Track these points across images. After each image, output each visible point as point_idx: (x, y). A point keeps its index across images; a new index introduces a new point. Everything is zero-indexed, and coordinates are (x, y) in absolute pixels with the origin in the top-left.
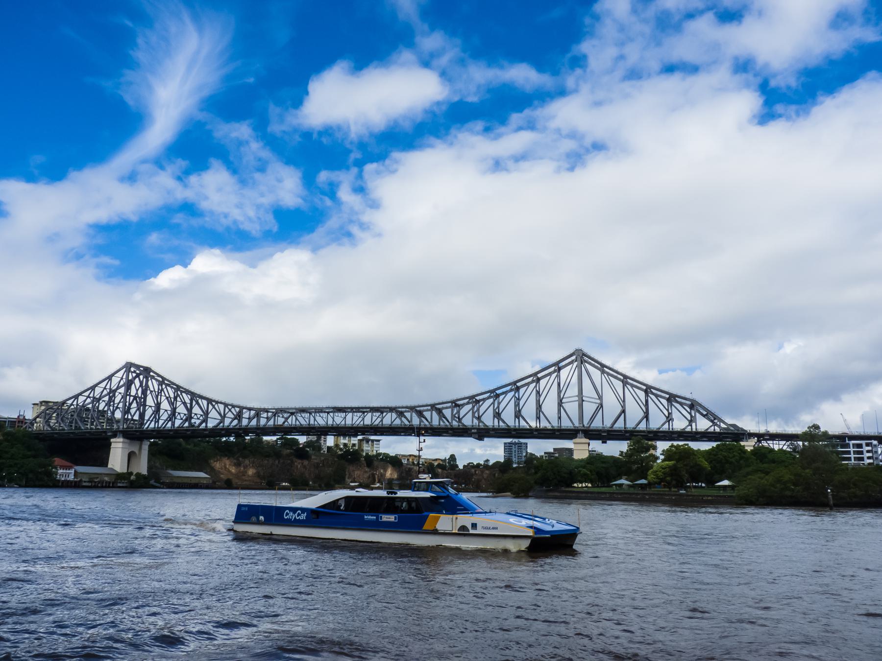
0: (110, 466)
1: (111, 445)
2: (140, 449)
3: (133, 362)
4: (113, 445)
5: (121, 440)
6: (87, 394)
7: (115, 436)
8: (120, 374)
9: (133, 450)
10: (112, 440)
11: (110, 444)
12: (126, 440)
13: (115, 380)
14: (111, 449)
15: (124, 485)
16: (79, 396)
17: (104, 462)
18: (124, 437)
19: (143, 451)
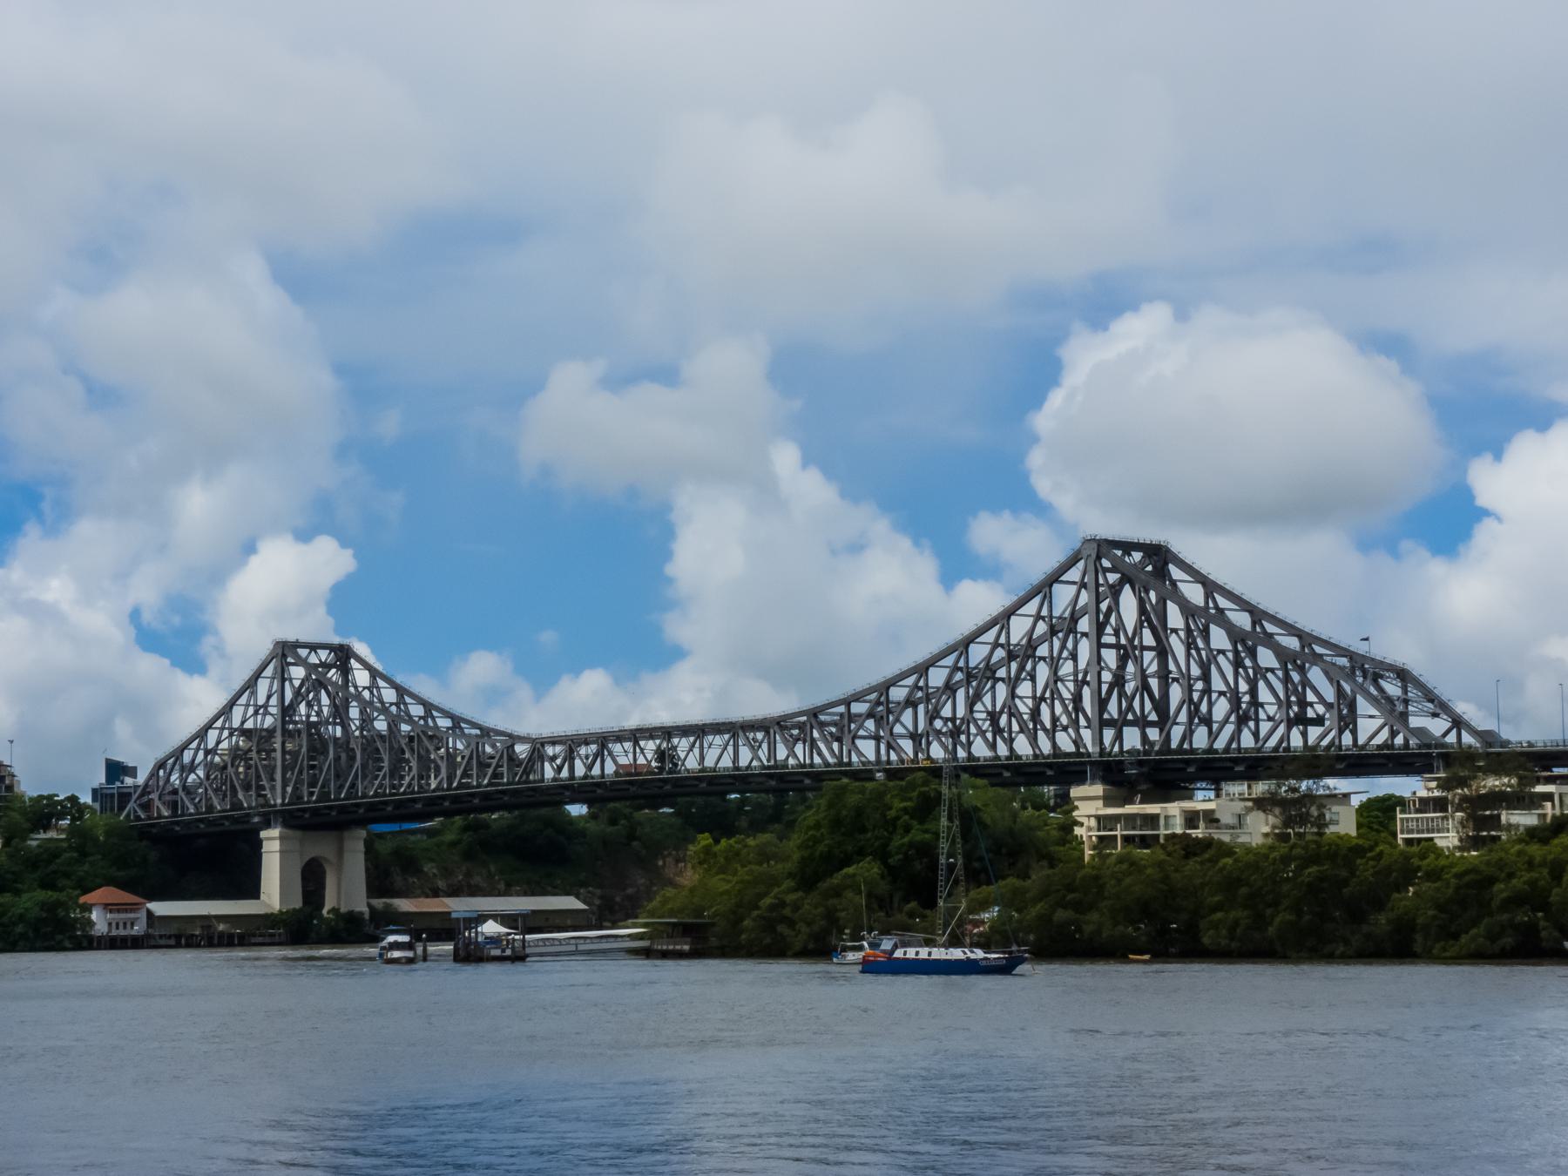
0: (263, 896)
1: (261, 848)
2: (340, 853)
3: (291, 638)
4: (266, 846)
5: (275, 832)
6: (219, 724)
7: (267, 825)
8: (269, 671)
9: (313, 855)
10: (263, 834)
11: (258, 844)
12: (290, 832)
13: (263, 687)
14: (264, 857)
15: (277, 939)
16: (207, 731)
17: (251, 889)
18: (286, 824)
19: (347, 856)
